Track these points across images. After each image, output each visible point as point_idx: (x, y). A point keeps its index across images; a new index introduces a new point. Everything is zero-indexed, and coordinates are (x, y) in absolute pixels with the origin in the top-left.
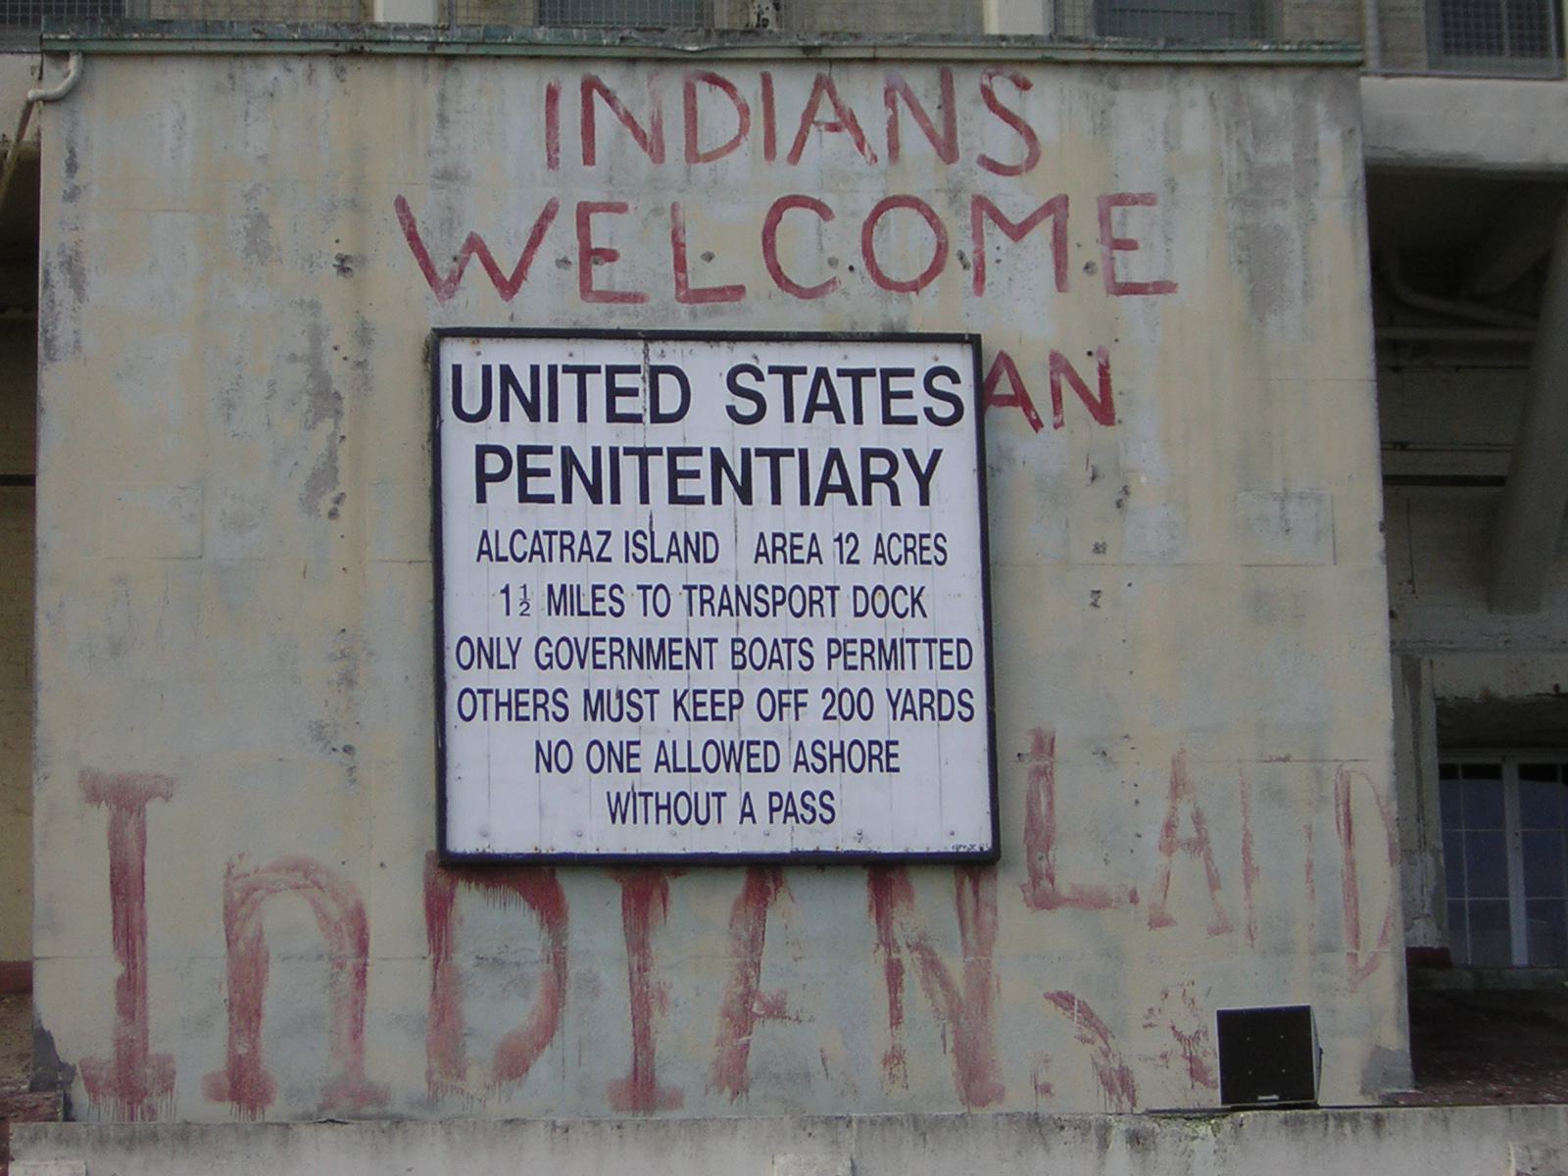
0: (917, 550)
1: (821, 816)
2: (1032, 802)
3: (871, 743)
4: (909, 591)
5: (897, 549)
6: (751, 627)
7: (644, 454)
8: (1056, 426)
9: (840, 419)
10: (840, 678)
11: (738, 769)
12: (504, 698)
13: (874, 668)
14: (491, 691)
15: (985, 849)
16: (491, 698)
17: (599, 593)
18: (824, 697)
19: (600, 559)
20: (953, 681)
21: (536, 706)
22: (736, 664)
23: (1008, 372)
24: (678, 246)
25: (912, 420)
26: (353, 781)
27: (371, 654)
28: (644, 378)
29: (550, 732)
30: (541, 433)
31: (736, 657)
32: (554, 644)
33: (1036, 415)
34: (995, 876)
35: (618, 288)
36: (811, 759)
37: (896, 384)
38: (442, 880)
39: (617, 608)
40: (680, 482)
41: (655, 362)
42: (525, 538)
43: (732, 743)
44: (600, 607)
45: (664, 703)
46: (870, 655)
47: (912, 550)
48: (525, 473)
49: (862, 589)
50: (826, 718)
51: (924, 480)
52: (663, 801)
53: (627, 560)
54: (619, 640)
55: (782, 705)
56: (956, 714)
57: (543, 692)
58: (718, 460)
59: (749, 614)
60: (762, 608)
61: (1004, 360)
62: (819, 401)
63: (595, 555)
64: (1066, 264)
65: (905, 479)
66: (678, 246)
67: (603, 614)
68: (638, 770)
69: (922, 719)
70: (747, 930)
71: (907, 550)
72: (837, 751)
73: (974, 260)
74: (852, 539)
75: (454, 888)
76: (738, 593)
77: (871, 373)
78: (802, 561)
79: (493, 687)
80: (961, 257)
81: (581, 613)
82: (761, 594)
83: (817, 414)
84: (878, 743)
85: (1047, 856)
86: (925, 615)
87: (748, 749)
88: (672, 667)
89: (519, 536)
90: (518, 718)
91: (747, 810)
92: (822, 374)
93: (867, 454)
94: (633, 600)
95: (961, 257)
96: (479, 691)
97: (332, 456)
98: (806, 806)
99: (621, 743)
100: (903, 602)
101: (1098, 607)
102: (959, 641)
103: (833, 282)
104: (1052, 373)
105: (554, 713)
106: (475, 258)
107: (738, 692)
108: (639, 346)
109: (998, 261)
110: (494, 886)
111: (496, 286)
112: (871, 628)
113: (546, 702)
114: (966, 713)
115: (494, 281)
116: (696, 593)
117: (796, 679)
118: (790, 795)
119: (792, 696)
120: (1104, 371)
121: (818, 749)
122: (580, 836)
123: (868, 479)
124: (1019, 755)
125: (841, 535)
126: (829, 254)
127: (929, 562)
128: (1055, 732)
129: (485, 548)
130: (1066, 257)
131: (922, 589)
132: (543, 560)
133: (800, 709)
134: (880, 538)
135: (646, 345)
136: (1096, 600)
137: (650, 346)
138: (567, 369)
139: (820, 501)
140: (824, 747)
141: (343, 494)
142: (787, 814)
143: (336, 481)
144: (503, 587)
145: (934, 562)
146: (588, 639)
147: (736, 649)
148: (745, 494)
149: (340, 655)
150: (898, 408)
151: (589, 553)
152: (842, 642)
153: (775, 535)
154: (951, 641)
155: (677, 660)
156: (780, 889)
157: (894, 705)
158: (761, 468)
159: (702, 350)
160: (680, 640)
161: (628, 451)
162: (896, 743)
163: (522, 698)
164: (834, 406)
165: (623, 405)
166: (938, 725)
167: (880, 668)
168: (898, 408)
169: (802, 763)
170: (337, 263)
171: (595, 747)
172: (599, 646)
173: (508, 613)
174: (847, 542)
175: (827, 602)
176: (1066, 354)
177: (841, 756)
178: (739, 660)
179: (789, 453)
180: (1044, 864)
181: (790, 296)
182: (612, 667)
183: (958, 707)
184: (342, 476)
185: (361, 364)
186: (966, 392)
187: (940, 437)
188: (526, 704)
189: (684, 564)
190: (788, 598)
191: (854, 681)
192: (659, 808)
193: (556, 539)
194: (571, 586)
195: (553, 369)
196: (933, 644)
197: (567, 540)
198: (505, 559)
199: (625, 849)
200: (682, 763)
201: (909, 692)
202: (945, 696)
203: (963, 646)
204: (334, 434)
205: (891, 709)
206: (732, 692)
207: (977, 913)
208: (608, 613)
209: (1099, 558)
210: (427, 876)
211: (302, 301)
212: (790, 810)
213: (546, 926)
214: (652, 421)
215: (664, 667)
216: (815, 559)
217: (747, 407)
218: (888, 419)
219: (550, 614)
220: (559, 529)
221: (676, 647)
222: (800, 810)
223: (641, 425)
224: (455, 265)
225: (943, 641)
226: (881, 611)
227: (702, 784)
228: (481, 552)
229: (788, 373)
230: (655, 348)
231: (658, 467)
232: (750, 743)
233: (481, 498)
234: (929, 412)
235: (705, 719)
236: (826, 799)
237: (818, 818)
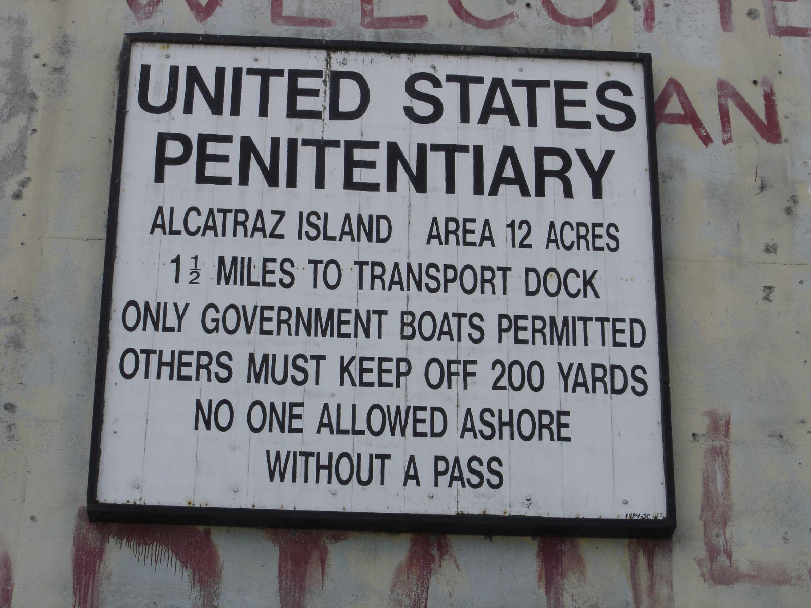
0: (590, 237)
1: (488, 481)
2: (707, 481)
3: (542, 413)
4: (581, 274)
5: (570, 236)
6: (420, 301)
7: (321, 146)
9: (514, 121)
10: (508, 350)
11: (403, 433)
12: (166, 358)
14: (154, 352)
15: (660, 518)
16: (154, 358)
17: (270, 266)
18: (493, 368)
19: (272, 235)
20: (627, 357)
21: (199, 367)
22: (405, 334)
23: (678, 96)
25: (585, 125)
26: (11, 438)
27: (40, 320)
28: (325, 81)
29: (211, 391)
30: (223, 124)
31: (405, 327)
32: (222, 310)
33: (706, 131)
34: (670, 550)
35: (307, 15)
36: (479, 426)
37: (569, 94)
38: (92, 536)
39: (287, 280)
40: (356, 171)
41: (336, 67)
42: (199, 214)
43: (398, 408)
44: (269, 278)
45: (330, 368)
46: (541, 331)
47: (584, 237)
48: (204, 157)
49: (534, 270)
50: (495, 387)
51: (596, 177)
52: (324, 461)
53: (300, 237)
55: (450, 374)
56: (629, 388)
57: (208, 354)
58: (394, 152)
59: (419, 289)
60: (433, 284)
61: (674, 85)
63: (268, 232)
64: (730, 9)
65: (578, 175)
67: (273, 285)
68: (299, 431)
69: (594, 391)
70: (409, 597)
71: (579, 237)
72: (506, 418)
73: (644, 4)
74: (524, 227)
75: (104, 544)
76: (409, 269)
77: (545, 84)
78: (474, 244)
81: (250, 283)
82: (432, 271)
83: (503, 188)
84: (548, 413)
86: (597, 296)
88: (340, 335)
89: (193, 214)
90: (180, 378)
91: (412, 472)
92: (498, 83)
93: (540, 153)
94: (303, 274)
96: (143, 351)
97: (21, 145)
99: (284, 404)
100: (575, 283)
102: (632, 321)
103: (511, 16)
104: (719, 97)
107: (406, 360)
108: (323, 54)
110: (145, 543)
111: (192, 10)
112: (543, 305)
114: (639, 387)
116: (367, 270)
117: (466, 350)
118: (457, 460)
119: (461, 367)
120: (769, 98)
121: (487, 416)
122: (236, 492)
123: (541, 174)
124: (694, 435)
125: (513, 222)
127: (602, 249)
128: (730, 414)
131: (595, 272)
133: (469, 379)
134: (552, 225)
135: (329, 55)
136: (768, 295)
137: (333, 55)
138: (251, 72)
139: (494, 191)
140: (493, 415)
141: (29, 178)
142: (453, 478)
143: (23, 167)
144: (174, 257)
145: (606, 248)
146: (256, 307)
147: (405, 321)
148: (419, 182)
149: (9, 320)
150: (571, 114)
151: (263, 230)
152: (513, 318)
153: (448, 220)
154: (623, 320)
155: (345, 329)
156: (446, 557)
157: (566, 378)
158: (436, 163)
159: (382, 60)
160: (349, 311)
161: (306, 142)
162: (567, 414)
163: (185, 359)
164: (509, 110)
165: (303, 103)
167: (552, 343)
168: (571, 114)
169: (469, 430)
171: (257, 409)
172: (267, 314)
173: (177, 281)
174: (520, 228)
175: (498, 281)
177: (510, 424)
178: (408, 331)
179: (465, 149)
180: (722, 539)
181: (469, 26)
182: (278, 334)
183: (631, 382)
184: (29, 163)
185: (59, 70)
186: (637, 103)
187: (612, 140)
189: (356, 242)
190: (459, 276)
191: (525, 354)
192: (319, 467)
193: (230, 217)
194: (243, 259)
195: (237, 73)
196: (606, 323)
197: (241, 218)
199: (282, 507)
200: (346, 424)
201: (580, 366)
202: (618, 373)
203: (636, 326)
204: (26, 128)
205: (562, 381)
206: (400, 360)
207: (652, 587)
208: (278, 284)
209: (771, 257)
210: (78, 529)
211: (10, 18)
212: (456, 474)
213: (197, 588)
215: (332, 336)
216: (487, 243)
217: (425, 109)
218: (561, 122)
219: (219, 283)
220: (234, 208)
221: (344, 317)
222: (467, 474)
223: (320, 121)
225: (616, 320)
226: (553, 290)
227: (366, 446)
228: (155, 225)
229: (465, 82)
230: (337, 57)
231: (335, 159)
232: (416, 409)
233: (159, 177)
234: (601, 119)
235: (371, 384)
236: (495, 465)
237: (485, 481)
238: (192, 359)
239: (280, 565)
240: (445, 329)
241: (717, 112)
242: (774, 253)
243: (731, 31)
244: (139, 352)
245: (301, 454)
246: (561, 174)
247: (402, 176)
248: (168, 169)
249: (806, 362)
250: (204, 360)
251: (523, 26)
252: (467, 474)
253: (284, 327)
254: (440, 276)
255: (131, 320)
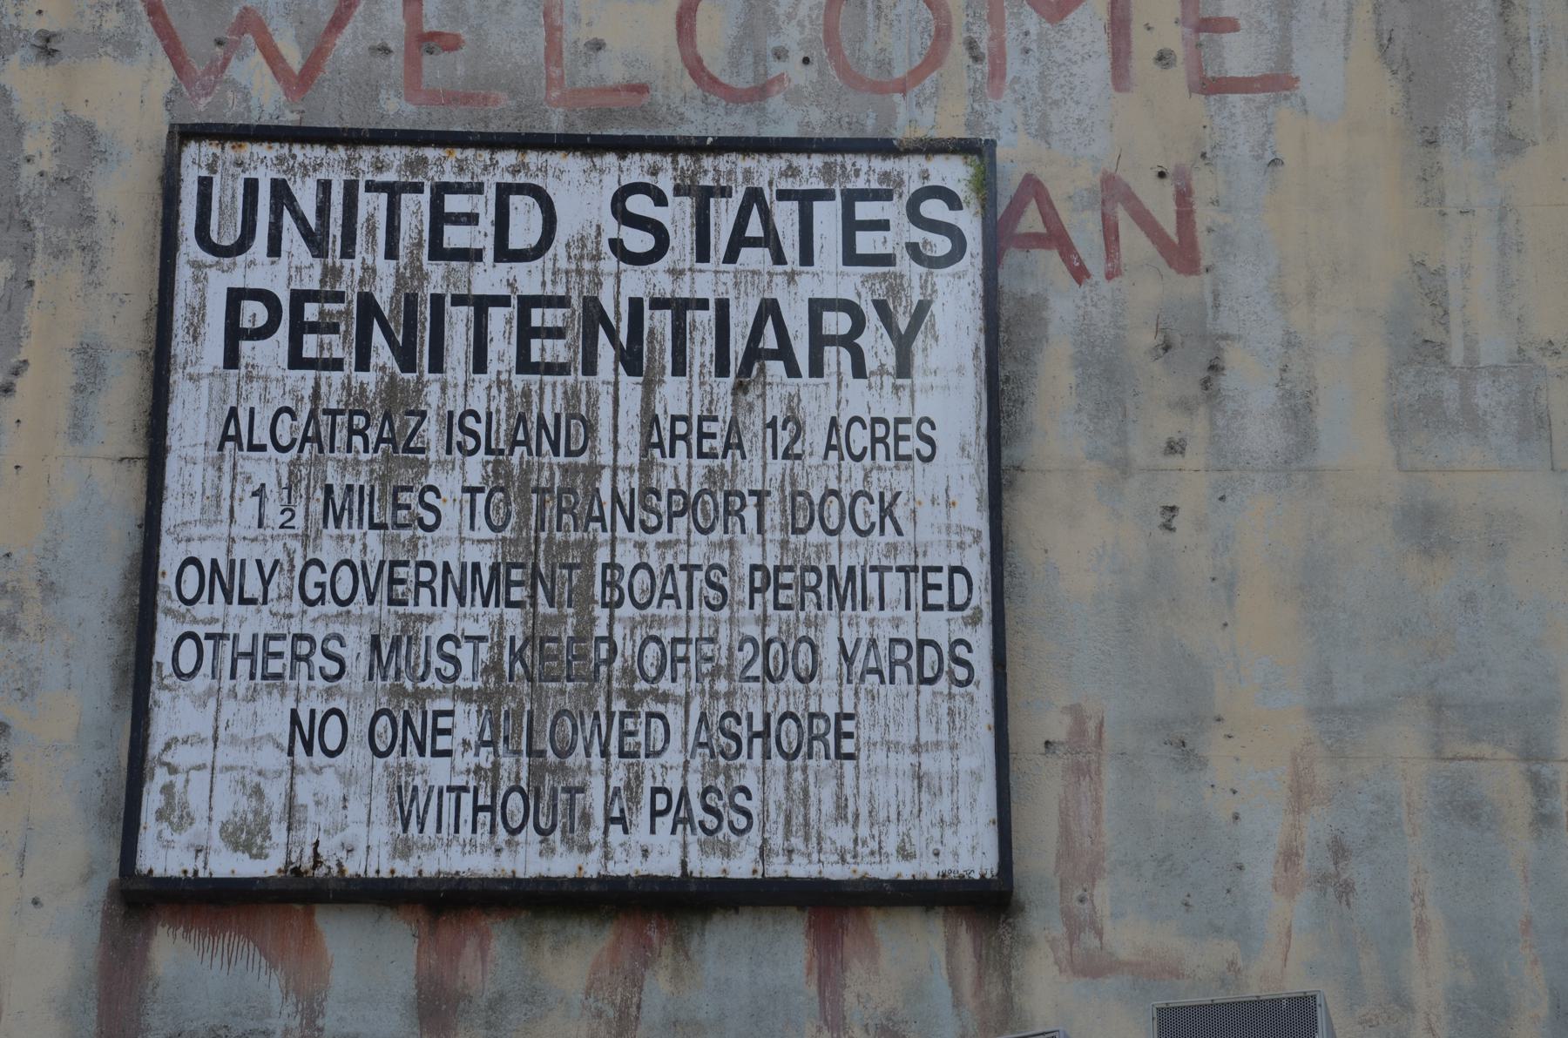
0: (891, 440)
5: (860, 438)
7: (482, 305)
8: (1109, 276)
11: (605, 753)
12: (244, 646)
13: (819, 607)
15: (988, 876)
19: (407, 449)
21: (296, 658)
24: (553, 31)
32: (330, 570)
39: (429, 518)
40: (535, 344)
42: (294, 417)
47: (883, 440)
48: (299, 328)
54: (429, 565)
59: (631, 529)
61: (1033, 187)
62: (748, 234)
64: (1128, 53)
65: (877, 345)
66: (553, 31)
68: (448, 753)
70: (613, 1004)
71: (875, 440)
72: (758, 726)
79: (231, 631)
80: (971, 45)
85: (1092, 895)
86: (899, 532)
87: (622, 724)
91: (616, 813)
93: (817, 308)
95: (971, 45)
96: (208, 636)
98: (708, 809)
100: (867, 512)
101: (1172, 530)
102: (954, 570)
103: (780, 78)
104: (1103, 202)
105: (321, 669)
106: (249, 39)
109: (1027, 51)
113: (312, 652)
115: (275, 74)
118: (684, 793)
119: (692, 648)
120: (1184, 198)
123: (818, 341)
124: (1047, 743)
125: (775, 418)
126: (773, 43)
127: (908, 458)
129: (232, 431)
130: (1129, 43)
132: (321, 450)
146: (382, 563)
150: (866, 242)
155: (517, 594)
159: (574, 164)
162: (850, 717)
163: (274, 646)
164: (770, 240)
166: (918, 692)
168: (866, 242)
170: (39, 43)
174: (784, 428)
175: (750, 514)
176: (1127, 176)
179: (703, 304)
186: (969, 222)
188: (279, 655)
192: (477, 809)
195: (350, 189)
198: (262, 448)
202: (929, 652)
203: (958, 578)
204: (14, 278)
209: (1176, 461)
213: (292, 998)
214: (498, 259)
217: (640, 242)
218: (851, 257)
222: (698, 813)
224: (219, 51)
228: (225, 437)
234: (914, 250)
237: (725, 824)
238: (284, 646)
239: (418, 957)
240: (669, 590)
241: (1100, 227)
242: (1181, 453)
243: (1127, 90)
244: (202, 637)
245: (450, 789)
246: (848, 341)
247: (606, 353)
248: (245, 346)
249: (1226, 625)
250: (304, 647)
251: (795, 97)
252: (698, 813)
253: (425, 593)
254: (663, 506)
255: (190, 589)
